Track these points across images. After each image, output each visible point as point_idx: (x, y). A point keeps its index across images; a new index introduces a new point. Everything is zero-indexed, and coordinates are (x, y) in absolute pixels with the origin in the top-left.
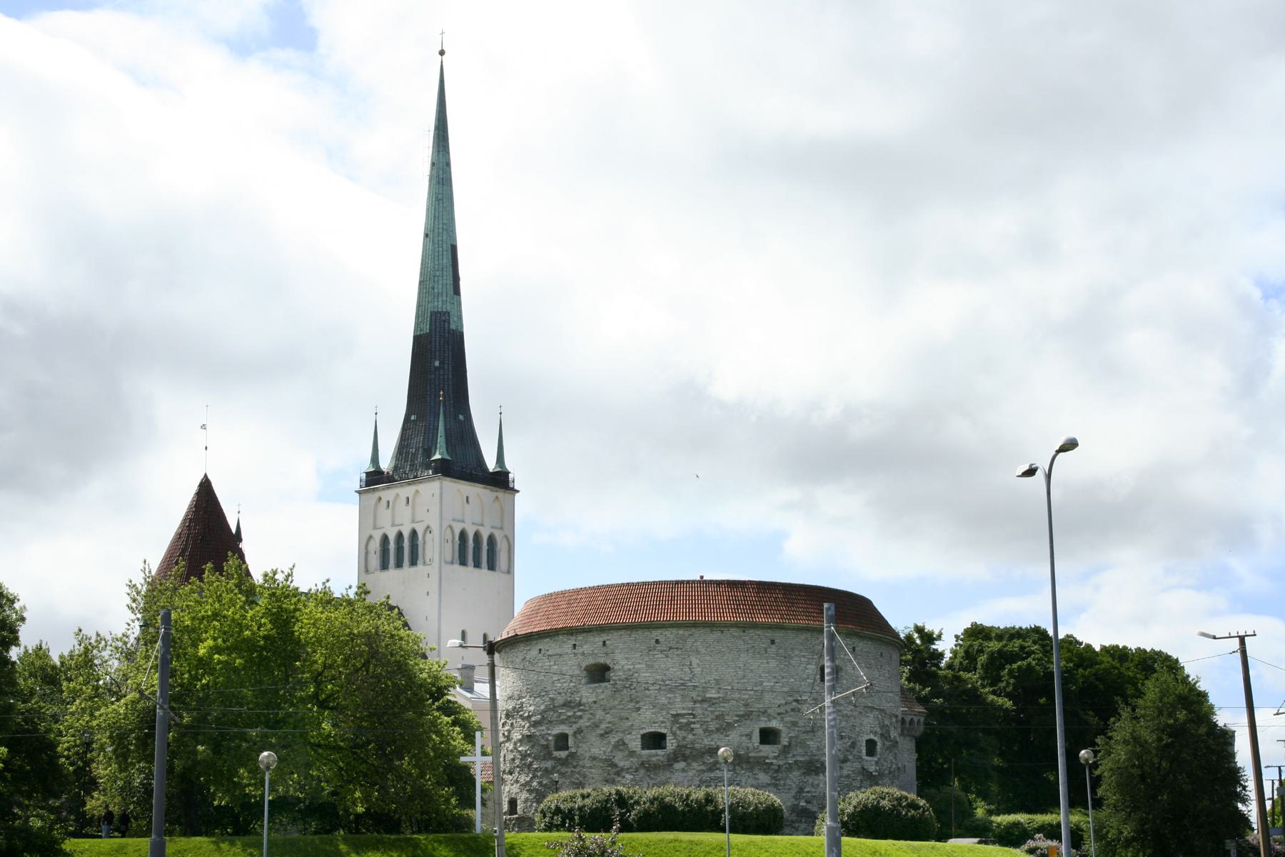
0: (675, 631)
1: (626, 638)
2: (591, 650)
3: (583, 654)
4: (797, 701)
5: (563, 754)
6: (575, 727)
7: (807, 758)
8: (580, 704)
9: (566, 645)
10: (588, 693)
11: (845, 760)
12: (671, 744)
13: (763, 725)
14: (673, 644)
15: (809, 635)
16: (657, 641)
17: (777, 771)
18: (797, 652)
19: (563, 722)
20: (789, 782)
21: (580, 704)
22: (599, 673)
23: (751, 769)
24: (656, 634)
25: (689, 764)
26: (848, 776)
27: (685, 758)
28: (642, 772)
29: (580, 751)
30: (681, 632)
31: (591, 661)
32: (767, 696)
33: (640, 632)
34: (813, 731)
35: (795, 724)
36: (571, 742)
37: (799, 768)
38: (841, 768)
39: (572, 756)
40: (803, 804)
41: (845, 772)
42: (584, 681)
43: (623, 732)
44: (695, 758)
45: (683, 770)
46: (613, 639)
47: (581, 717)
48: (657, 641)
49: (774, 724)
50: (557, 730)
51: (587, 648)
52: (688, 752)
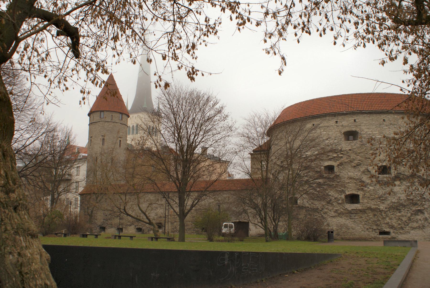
0: (392, 115)
1: (367, 118)
2: (347, 123)
3: (342, 126)
5: (332, 176)
6: (338, 162)
8: (341, 150)
9: (332, 122)
10: (345, 145)
12: (393, 172)
14: (392, 122)
16: (384, 120)
19: (330, 160)
21: (341, 150)
22: (351, 135)
24: (383, 116)
25: (401, 183)
27: (400, 180)
28: (378, 186)
29: (341, 175)
30: (396, 116)
31: (347, 129)
33: (375, 115)
36: (336, 169)
39: (337, 176)
42: (343, 139)
43: (367, 165)
44: (404, 179)
45: (399, 186)
46: (360, 119)
47: (342, 157)
48: (384, 120)
50: (327, 164)
51: (345, 123)
52: (401, 176)
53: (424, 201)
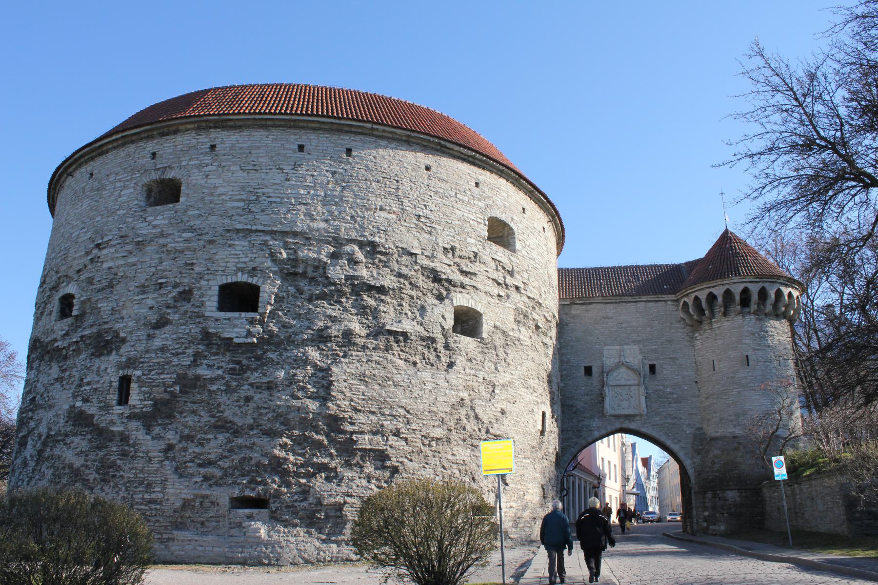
4: (98, 246)
7: (94, 330)
11: (162, 323)
13: (61, 293)
15: (131, 148)
17: (66, 358)
18: (112, 179)
20: (74, 373)
23: (51, 360)
26: (163, 349)
32: (72, 251)
34: (111, 286)
35: (90, 281)
37: (87, 346)
38: (150, 337)
40: (79, 404)
41: (157, 343)
49: (71, 289)
53: (32, 410)
